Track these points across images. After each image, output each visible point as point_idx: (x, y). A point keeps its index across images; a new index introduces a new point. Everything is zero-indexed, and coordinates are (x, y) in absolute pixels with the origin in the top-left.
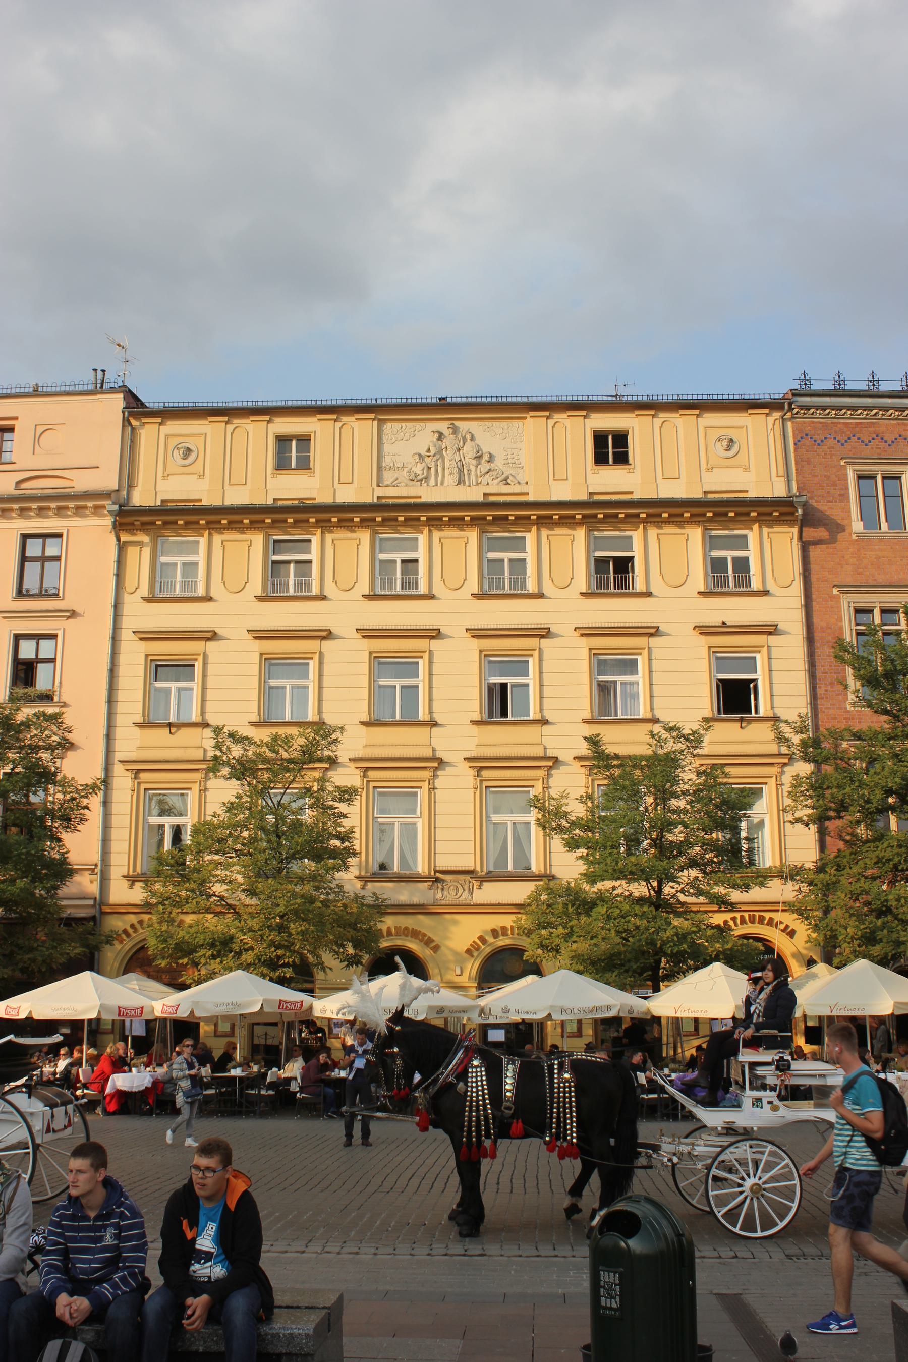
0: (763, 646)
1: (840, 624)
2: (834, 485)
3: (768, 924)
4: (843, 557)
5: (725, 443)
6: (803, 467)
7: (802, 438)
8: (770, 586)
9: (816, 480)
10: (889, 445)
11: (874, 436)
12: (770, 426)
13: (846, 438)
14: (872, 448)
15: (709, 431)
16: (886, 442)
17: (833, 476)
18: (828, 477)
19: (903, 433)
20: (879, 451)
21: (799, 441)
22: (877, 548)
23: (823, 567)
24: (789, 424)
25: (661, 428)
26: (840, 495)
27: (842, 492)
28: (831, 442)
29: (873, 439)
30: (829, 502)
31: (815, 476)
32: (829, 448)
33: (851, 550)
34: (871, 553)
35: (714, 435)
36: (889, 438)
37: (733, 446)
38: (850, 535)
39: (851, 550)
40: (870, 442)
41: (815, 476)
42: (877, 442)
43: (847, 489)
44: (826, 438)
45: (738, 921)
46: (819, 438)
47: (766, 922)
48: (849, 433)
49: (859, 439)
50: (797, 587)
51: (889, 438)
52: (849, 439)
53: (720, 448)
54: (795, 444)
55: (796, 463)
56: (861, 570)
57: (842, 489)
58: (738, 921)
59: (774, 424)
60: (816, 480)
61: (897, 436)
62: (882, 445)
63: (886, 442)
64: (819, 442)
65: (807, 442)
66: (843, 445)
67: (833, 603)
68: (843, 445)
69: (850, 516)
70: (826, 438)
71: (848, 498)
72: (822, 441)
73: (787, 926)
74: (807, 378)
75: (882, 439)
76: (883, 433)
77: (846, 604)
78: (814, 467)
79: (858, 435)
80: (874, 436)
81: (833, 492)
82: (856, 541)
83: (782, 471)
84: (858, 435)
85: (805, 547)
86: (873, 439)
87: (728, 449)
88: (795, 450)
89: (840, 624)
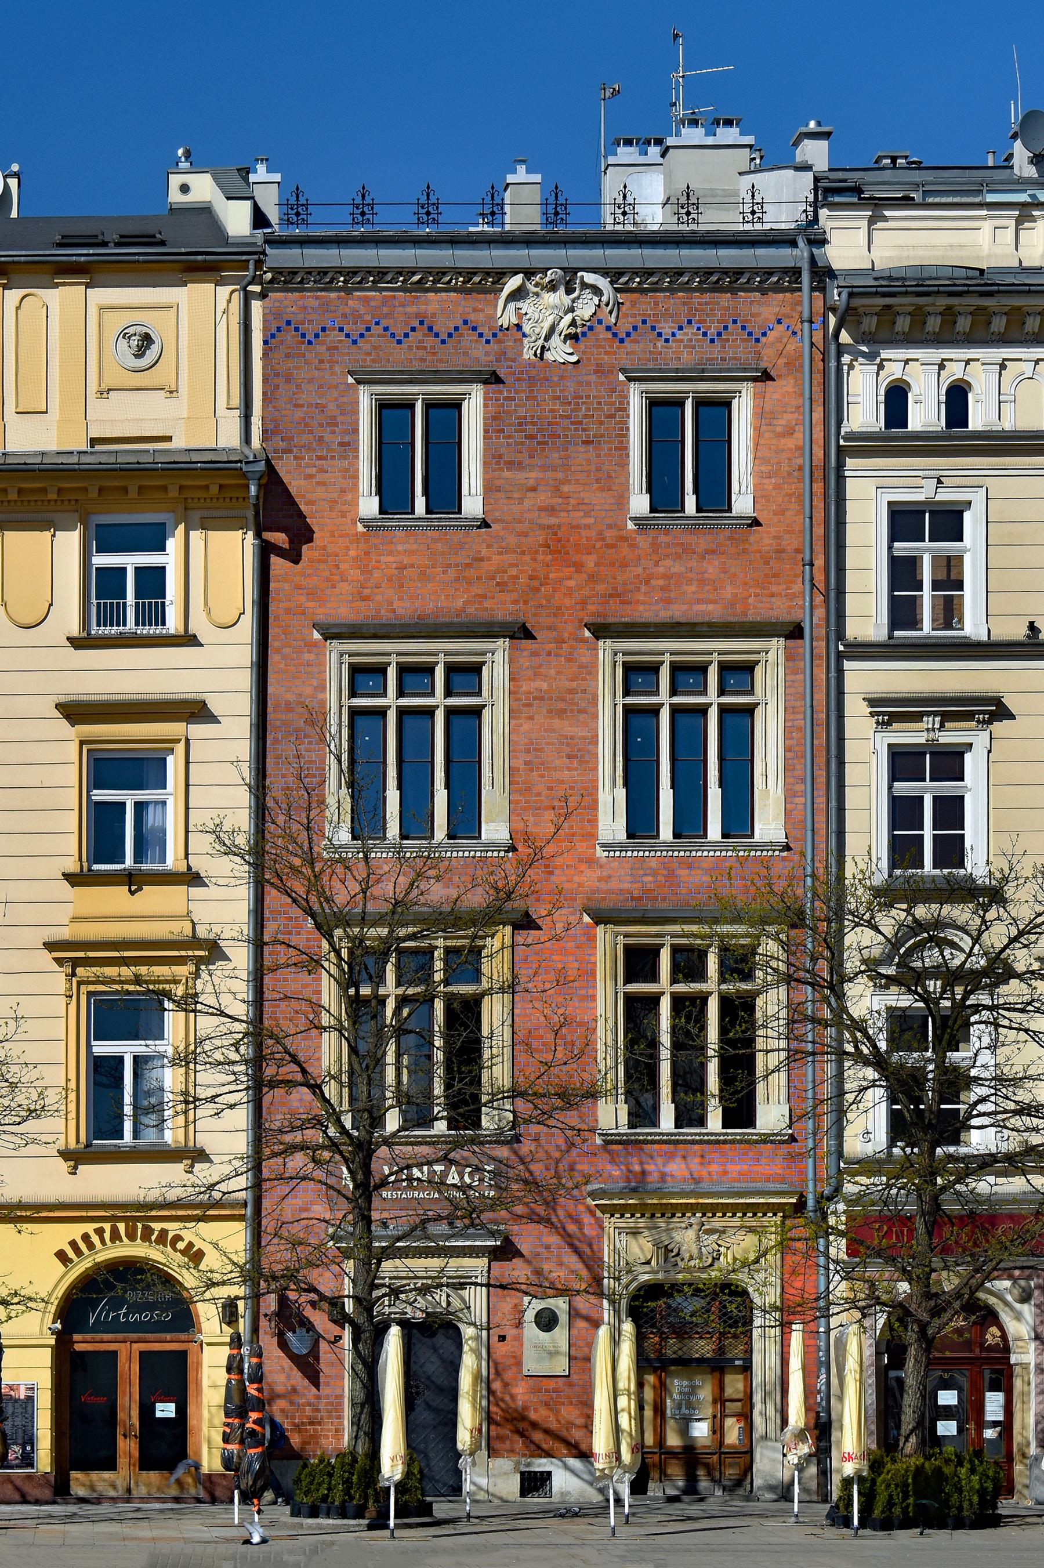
0: (178, 741)
1: (320, 696)
2: (333, 423)
3: (157, 1241)
4: (337, 567)
5: (134, 343)
6: (277, 387)
7: (279, 329)
8: (199, 626)
9: (299, 414)
10: (443, 342)
11: (416, 324)
12: (222, 305)
13: (361, 328)
14: (410, 348)
15: (107, 315)
16: (437, 335)
17: (332, 406)
18: (322, 408)
19: (472, 317)
20: (421, 353)
21: (273, 336)
22: (400, 548)
23: (298, 587)
24: (256, 306)
25: (18, 308)
26: (341, 444)
27: (347, 439)
28: (334, 336)
29: (413, 329)
30: (319, 458)
31: (297, 406)
32: (329, 349)
33: (352, 553)
34: (390, 559)
35: (117, 322)
36: (443, 326)
37: (148, 347)
38: (354, 523)
39: (352, 553)
40: (406, 335)
41: (297, 406)
42: (419, 335)
43: (356, 431)
44: (324, 329)
45: (107, 1236)
46: (310, 329)
47: (153, 1238)
48: (368, 318)
49: (386, 329)
50: (246, 629)
51: (443, 326)
52: (368, 329)
53: (125, 350)
54: (265, 342)
55: (265, 380)
56: (367, 592)
57: (346, 432)
58: (107, 1236)
59: (229, 301)
60: (299, 414)
61: (460, 323)
62: (430, 342)
63: (437, 335)
64: (310, 337)
65: (289, 337)
66: (355, 342)
67: (311, 657)
68: (355, 342)
69: (356, 486)
70: (324, 329)
71: (357, 450)
72: (317, 336)
73: (191, 1245)
74: (302, 201)
75: (430, 329)
76: (434, 315)
77: (334, 656)
78: (299, 387)
79: (384, 323)
80: (416, 324)
81: (328, 437)
82: (363, 534)
83: (236, 400)
84: (384, 323)
85: (265, 552)
86: (413, 329)
87: (140, 354)
88: (265, 355)
89: (320, 696)
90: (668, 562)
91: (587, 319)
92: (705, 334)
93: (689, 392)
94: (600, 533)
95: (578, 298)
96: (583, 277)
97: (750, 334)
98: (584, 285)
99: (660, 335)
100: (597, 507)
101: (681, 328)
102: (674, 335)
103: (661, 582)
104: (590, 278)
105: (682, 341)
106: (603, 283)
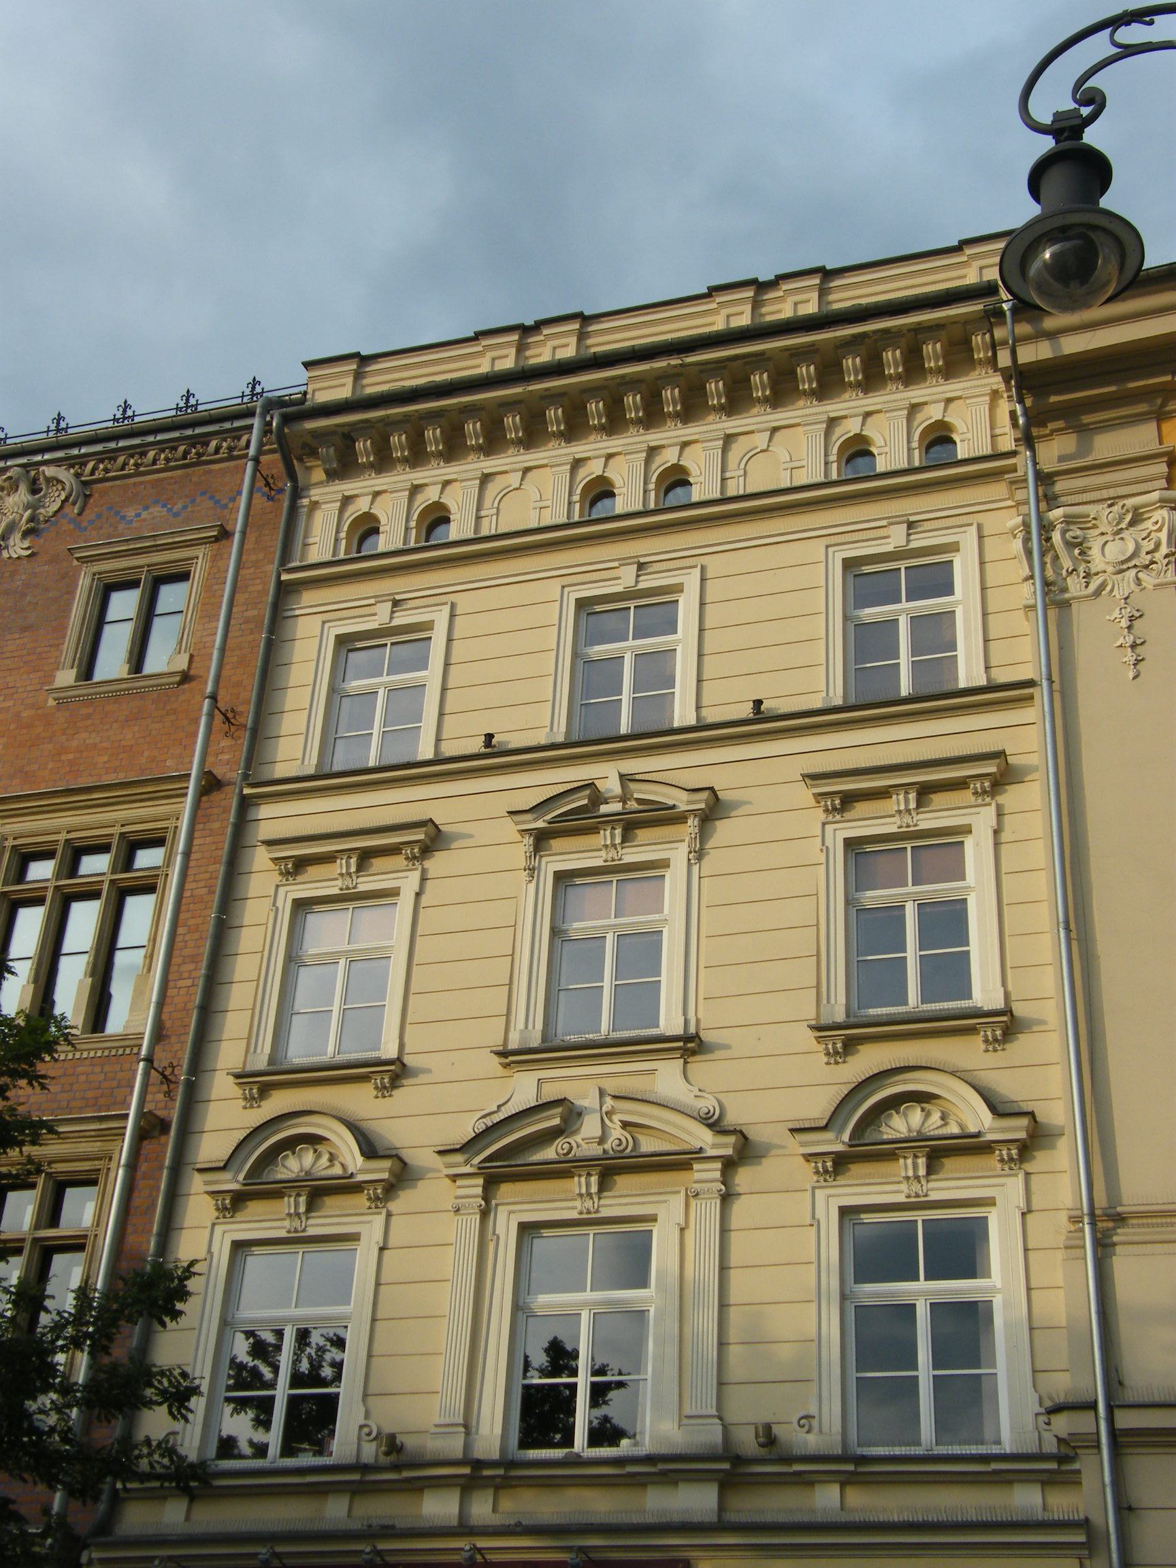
90: (84, 735)
91: (50, 514)
92: (170, 510)
93: (142, 567)
94: (18, 714)
95: (45, 496)
96: (43, 472)
97: (218, 502)
98: (48, 480)
99: (124, 518)
100: (20, 690)
101: (146, 508)
102: (138, 515)
103: (71, 756)
104: (50, 471)
105: (144, 520)
106: (65, 475)
